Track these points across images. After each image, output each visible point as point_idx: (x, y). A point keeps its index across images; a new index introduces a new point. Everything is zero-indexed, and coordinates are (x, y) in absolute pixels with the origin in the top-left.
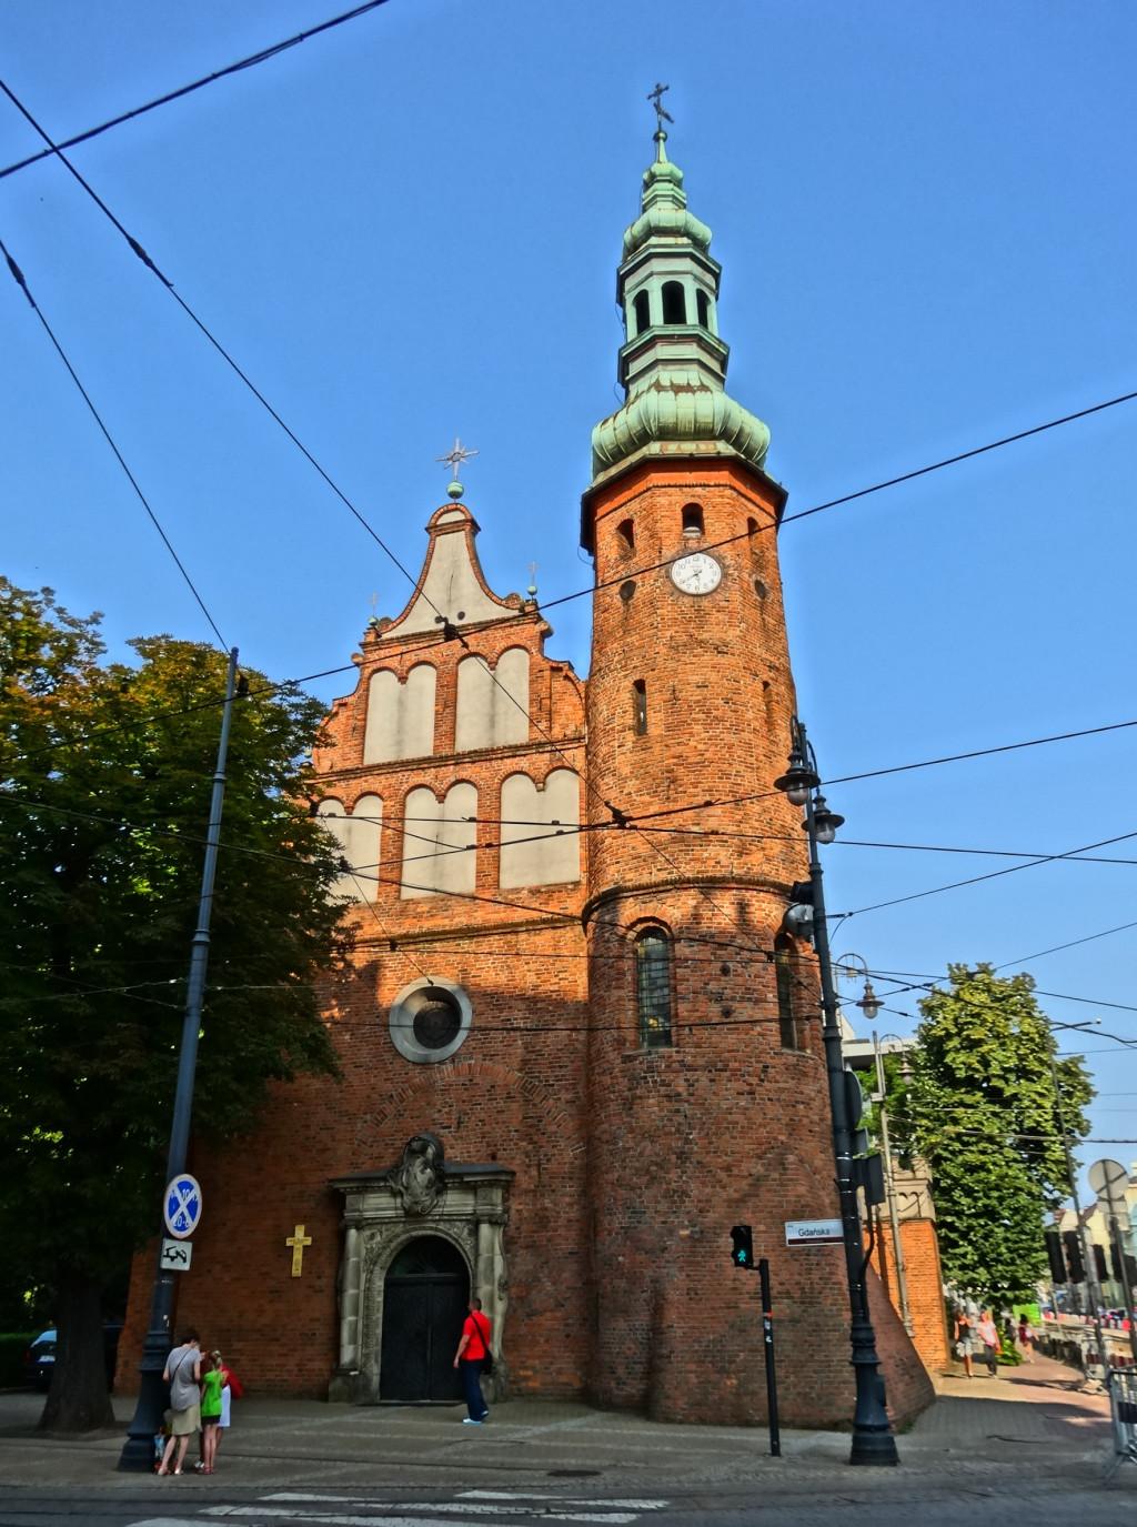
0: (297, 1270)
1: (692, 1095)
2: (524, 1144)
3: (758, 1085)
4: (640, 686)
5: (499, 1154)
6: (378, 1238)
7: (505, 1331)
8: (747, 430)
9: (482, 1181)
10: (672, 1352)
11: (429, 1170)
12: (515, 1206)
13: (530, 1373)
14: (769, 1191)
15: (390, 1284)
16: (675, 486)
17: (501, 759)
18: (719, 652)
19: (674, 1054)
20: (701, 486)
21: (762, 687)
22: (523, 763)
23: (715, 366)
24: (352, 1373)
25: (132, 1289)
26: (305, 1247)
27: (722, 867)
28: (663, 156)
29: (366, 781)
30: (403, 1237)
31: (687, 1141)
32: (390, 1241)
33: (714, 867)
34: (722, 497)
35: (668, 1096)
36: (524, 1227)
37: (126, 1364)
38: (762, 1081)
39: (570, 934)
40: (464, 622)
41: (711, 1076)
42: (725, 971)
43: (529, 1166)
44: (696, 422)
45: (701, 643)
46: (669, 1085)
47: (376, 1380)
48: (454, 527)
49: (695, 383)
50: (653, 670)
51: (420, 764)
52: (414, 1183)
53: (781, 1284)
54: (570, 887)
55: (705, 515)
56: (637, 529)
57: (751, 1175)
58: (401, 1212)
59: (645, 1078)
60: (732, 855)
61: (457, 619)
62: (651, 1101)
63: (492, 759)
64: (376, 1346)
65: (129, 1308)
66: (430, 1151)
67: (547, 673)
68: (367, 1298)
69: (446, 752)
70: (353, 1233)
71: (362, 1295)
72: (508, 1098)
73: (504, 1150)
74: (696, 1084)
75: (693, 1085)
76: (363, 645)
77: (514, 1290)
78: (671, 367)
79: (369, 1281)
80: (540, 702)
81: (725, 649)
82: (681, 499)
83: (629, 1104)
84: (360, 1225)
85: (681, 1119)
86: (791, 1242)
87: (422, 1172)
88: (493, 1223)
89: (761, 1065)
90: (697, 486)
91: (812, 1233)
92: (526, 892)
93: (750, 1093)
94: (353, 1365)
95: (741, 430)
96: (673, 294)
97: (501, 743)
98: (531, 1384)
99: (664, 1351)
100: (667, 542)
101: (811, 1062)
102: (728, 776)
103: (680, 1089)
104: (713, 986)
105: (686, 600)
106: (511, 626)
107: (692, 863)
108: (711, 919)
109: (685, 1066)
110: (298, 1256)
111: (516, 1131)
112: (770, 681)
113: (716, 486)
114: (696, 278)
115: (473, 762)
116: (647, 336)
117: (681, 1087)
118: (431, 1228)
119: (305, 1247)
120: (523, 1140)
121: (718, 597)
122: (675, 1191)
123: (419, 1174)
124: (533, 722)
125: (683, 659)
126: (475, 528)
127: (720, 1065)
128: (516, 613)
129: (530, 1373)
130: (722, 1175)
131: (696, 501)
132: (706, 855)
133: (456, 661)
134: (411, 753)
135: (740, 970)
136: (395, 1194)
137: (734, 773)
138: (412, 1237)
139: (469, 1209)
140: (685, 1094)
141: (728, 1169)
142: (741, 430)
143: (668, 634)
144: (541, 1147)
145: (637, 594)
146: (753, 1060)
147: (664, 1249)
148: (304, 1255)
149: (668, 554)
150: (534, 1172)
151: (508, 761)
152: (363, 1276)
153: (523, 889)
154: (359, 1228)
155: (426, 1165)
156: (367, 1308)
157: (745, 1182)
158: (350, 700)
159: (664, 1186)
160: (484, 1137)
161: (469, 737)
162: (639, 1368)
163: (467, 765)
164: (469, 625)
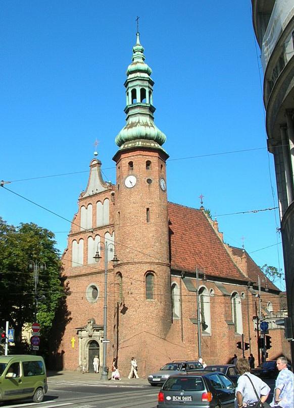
0: (73, 346)
4: (119, 212)
8: (148, 133)
23: (147, 111)
28: (138, 42)
40: (97, 192)
42: (131, 284)
48: (95, 165)
66: (92, 322)
95: (146, 134)
96: (134, 92)
110: (73, 343)
114: (140, 86)
126: (99, 164)
128: (107, 189)
142: (146, 134)
155: (91, 325)
161: (99, 224)
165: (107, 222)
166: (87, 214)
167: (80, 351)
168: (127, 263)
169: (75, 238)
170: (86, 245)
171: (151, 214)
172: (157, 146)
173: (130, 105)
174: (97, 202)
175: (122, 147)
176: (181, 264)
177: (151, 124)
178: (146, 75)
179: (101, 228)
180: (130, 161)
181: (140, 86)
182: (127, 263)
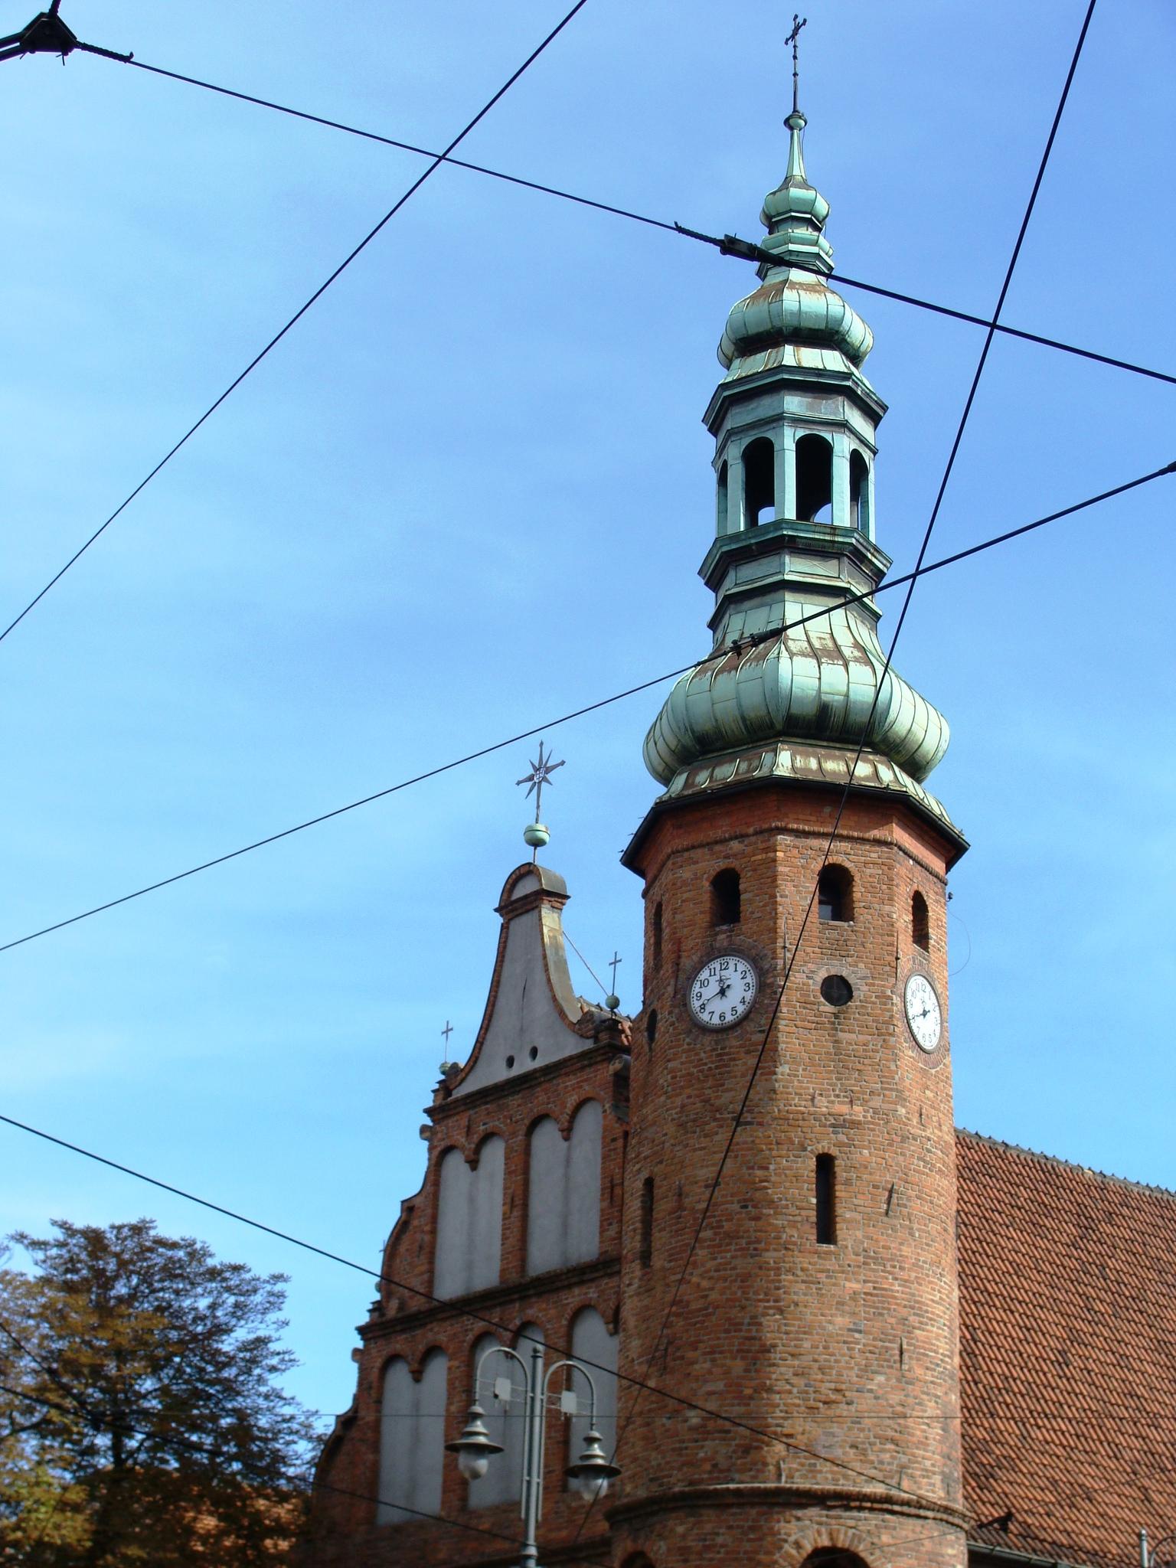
16: (701, 846)
17: (570, 1286)
20: (736, 838)
21: (812, 1163)
22: (592, 1293)
27: (721, 1471)
29: (431, 1330)
33: (710, 1472)
34: (767, 850)
40: (539, 1063)
44: (744, 719)
55: (742, 887)
60: (734, 1452)
61: (529, 1059)
63: (558, 1290)
69: (514, 1278)
76: (429, 1112)
78: (747, 604)
82: (709, 865)
90: (731, 839)
100: (688, 944)
102: (737, 1326)
105: (707, 1039)
106: (583, 1068)
107: (685, 1469)
108: (700, 1553)
113: (756, 833)
114: (798, 421)
115: (539, 1295)
121: (750, 1027)
125: (691, 1142)
128: (589, 1044)
131: (734, 864)
132: (702, 1455)
137: (747, 1321)
142: (824, 709)
143: (678, 1101)
149: (687, 963)
151: (576, 1291)
158: (417, 1202)
161: (543, 1257)
163: (534, 1300)
165: (586, 1245)
166: (472, 1200)
168: (694, 1501)
169: (399, 1344)
170: (464, 1387)
171: (840, 1191)
172: (889, 776)
173: (736, 537)
175: (679, 782)
176: (1049, 1522)
177: (857, 645)
178: (833, 360)
180: (722, 864)
181: (798, 421)
182: (694, 1501)
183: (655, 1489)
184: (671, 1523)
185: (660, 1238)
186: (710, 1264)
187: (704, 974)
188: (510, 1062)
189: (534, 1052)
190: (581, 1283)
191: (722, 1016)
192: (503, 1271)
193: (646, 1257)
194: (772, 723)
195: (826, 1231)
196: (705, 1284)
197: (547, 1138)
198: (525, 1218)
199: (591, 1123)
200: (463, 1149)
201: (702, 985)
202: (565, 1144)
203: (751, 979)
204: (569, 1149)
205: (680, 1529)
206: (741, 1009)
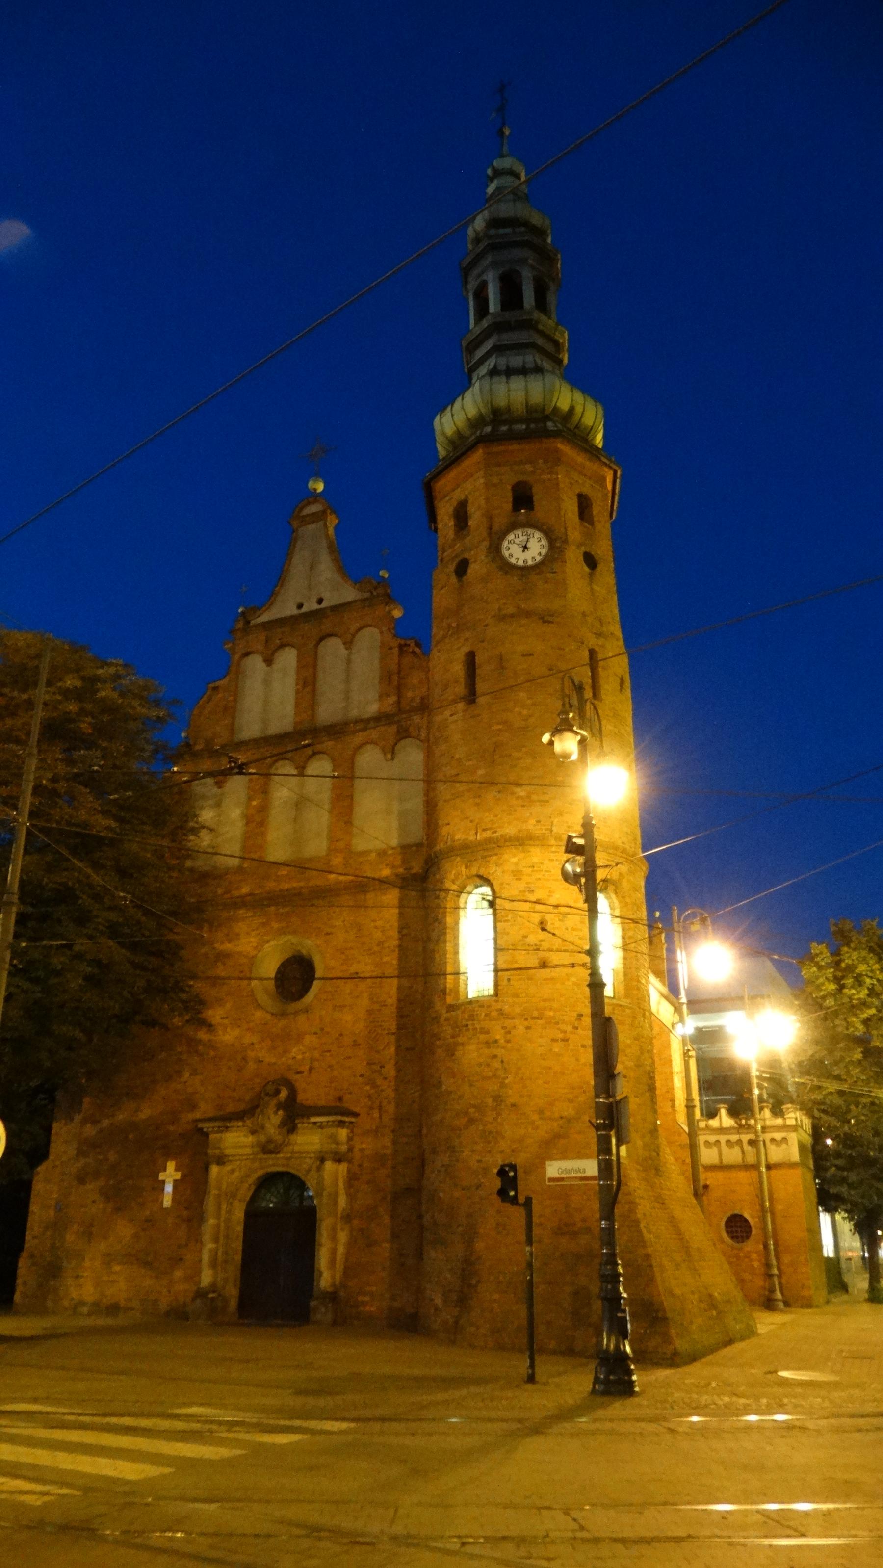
0: (167, 1202)
1: (508, 1041)
2: (368, 1088)
3: (571, 1033)
5: (347, 1097)
6: (237, 1174)
7: (347, 1260)
9: (328, 1122)
10: (479, 1282)
11: (281, 1112)
12: (358, 1146)
13: (367, 1299)
14: (579, 1133)
15: (252, 1216)
18: (544, 622)
19: (493, 1003)
22: (374, 734)
24: (211, 1295)
25: (30, 1219)
26: (175, 1181)
30: (260, 1173)
31: (503, 1085)
32: (248, 1176)
34: (551, 473)
35: (487, 1043)
36: (366, 1164)
37: (25, 1283)
38: (576, 1028)
39: (413, 893)
40: (323, 605)
41: (526, 1023)
43: (371, 1108)
44: (527, 403)
45: (528, 614)
46: (488, 1032)
47: (233, 1304)
49: (530, 365)
50: (483, 641)
51: (282, 738)
52: (267, 1125)
53: (584, 1220)
54: (414, 848)
55: (534, 490)
56: (471, 509)
57: (562, 1118)
58: (256, 1149)
59: (467, 1025)
62: (472, 1047)
64: (233, 1272)
65: (27, 1233)
66: (284, 1093)
67: (396, 651)
68: (227, 1228)
70: (214, 1170)
71: (222, 1224)
72: (353, 1045)
73: (350, 1093)
74: (514, 1032)
75: (509, 1032)
77: (356, 1222)
79: (229, 1212)
80: (389, 678)
81: (550, 619)
83: (451, 1052)
84: (221, 1160)
85: (496, 1064)
86: (551, 1180)
87: (276, 1113)
88: (339, 1160)
89: (575, 1014)
91: (570, 1171)
92: (374, 855)
93: (563, 1040)
94: (213, 1287)
97: (354, 713)
98: (368, 1308)
99: (474, 1282)
101: (628, 1011)
103: (498, 1037)
104: (532, 939)
109: (502, 1014)
110: (169, 1188)
111: (362, 1076)
112: (597, 649)
116: (485, 323)
117: (499, 1035)
118: (283, 1165)
119: (175, 1181)
120: (367, 1084)
122: (490, 1133)
123: (272, 1116)
124: (382, 696)
127: (535, 1014)
128: (367, 595)
129: (367, 1299)
130: (535, 1117)
133: (314, 642)
134: (275, 728)
135: (558, 924)
136: (253, 1132)
138: (267, 1173)
139: (317, 1147)
140: (502, 1041)
141: (541, 1112)
144: (382, 1091)
145: (469, 571)
146: (567, 1009)
147: (478, 1186)
148: (175, 1188)
150: (376, 1115)
152: (224, 1207)
153: (371, 851)
154: (218, 1163)
155: (279, 1106)
156: (227, 1237)
157: (555, 1124)
159: (481, 1128)
160: (331, 1083)
162: (454, 1296)
164: (325, 609)
166: (267, 682)
167: (212, 1221)
171: (602, 673)
174: (322, 639)
179: (337, 730)
180: (521, 478)
183: (488, 834)
184: (506, 856)
185: (480, 687)
186: (529, 701)
187: (511, 537)
188: (300, 606)
189: (320, 601)
190: (364, 729)
191: (525, 561)
192: (296, 723)
193: (471, 697)
194: (544, 409)
195: (596, 694)
196: (525, 712)
197: (333, 649)
198: (314, 691)
199: (370, 641)
200: (261, 653)
201: (509, 542)
202: (346, 652)
203: (544, 542)
204: (349, 655)
205: (514, 860)
206: (538, 559)
